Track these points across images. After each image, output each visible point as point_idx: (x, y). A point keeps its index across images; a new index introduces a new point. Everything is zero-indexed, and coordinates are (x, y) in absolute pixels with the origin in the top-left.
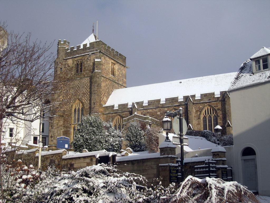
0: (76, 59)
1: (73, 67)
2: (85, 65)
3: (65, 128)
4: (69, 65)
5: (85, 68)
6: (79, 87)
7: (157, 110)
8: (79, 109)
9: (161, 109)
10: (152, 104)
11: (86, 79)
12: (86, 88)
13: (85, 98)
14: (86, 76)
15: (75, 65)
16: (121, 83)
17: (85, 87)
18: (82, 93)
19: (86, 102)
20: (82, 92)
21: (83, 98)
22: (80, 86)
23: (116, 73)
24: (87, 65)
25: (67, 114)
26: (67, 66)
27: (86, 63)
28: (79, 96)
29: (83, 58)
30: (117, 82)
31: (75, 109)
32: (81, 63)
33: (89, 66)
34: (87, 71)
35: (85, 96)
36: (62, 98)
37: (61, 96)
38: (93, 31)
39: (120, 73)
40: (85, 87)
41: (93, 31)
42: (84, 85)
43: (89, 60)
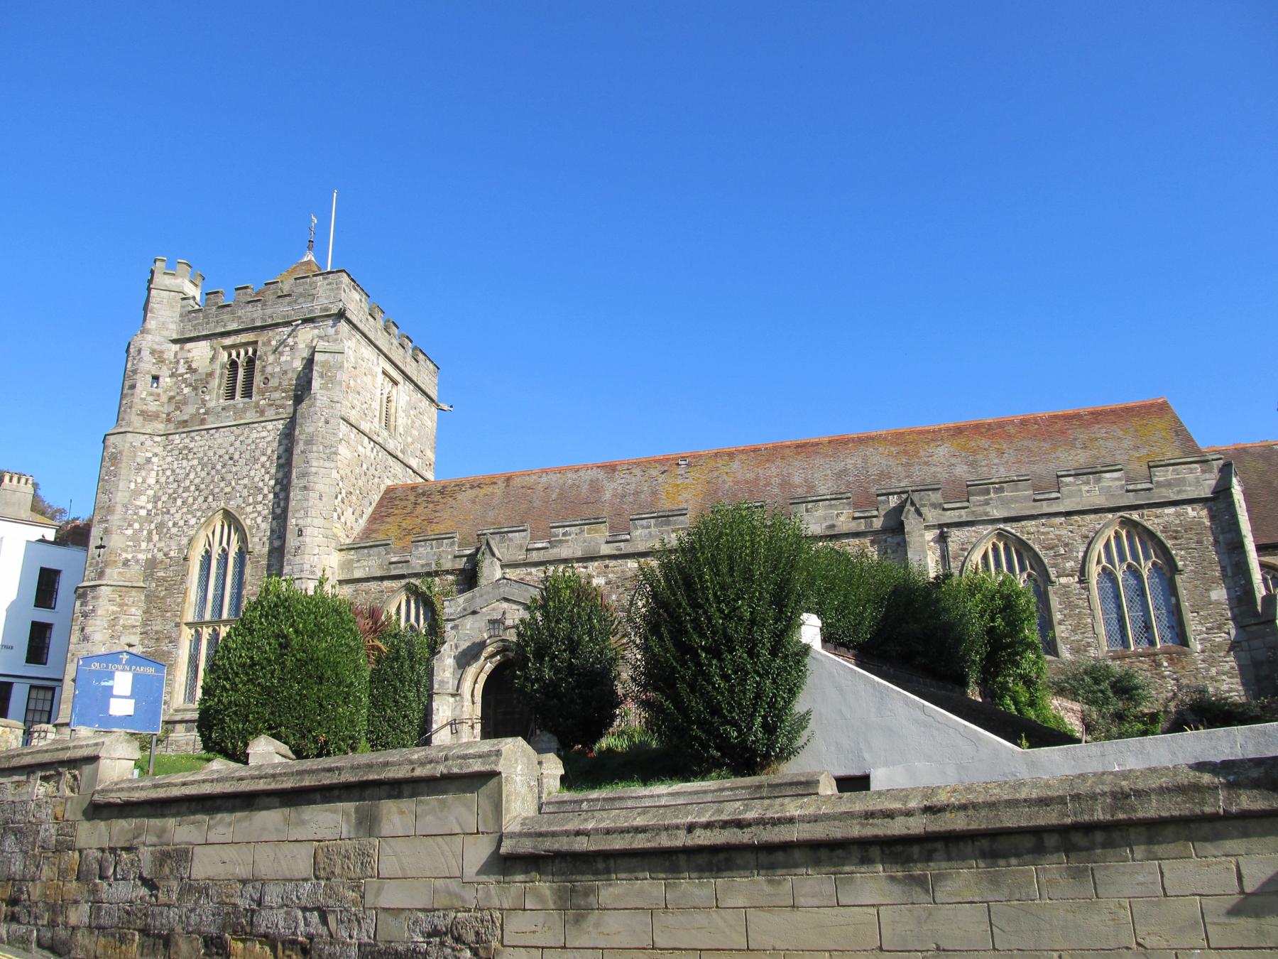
0: (228, 341)
1: (211, 375)
2: (269, 369)
3: (152, 643)
4: (194, 366)
6: (231, 459)
7: (593, 567)
9: (612, 563)
10: (567, 541)
13: (259, 508)
14: (270, 413)
15: (223, 367)
16: (414, 463)
17: (264, 459)
18: (245, 486)
20: (246, 481)
21: (249, 509)
22: (236, 456)
23: (400, 421)
24: (277, 369)
25: (164, 579)
26: (182, 370)
27: (271, 358)
29: (262, 338)
30: (400, 455)
31: (207, 556)
32: (251, 362)
33: (285, 372)
34: (277, 395)
35: (260, 498)
36: (150, 506)
37: (144, 498)
39: (413, 422)
42: (257, 453)
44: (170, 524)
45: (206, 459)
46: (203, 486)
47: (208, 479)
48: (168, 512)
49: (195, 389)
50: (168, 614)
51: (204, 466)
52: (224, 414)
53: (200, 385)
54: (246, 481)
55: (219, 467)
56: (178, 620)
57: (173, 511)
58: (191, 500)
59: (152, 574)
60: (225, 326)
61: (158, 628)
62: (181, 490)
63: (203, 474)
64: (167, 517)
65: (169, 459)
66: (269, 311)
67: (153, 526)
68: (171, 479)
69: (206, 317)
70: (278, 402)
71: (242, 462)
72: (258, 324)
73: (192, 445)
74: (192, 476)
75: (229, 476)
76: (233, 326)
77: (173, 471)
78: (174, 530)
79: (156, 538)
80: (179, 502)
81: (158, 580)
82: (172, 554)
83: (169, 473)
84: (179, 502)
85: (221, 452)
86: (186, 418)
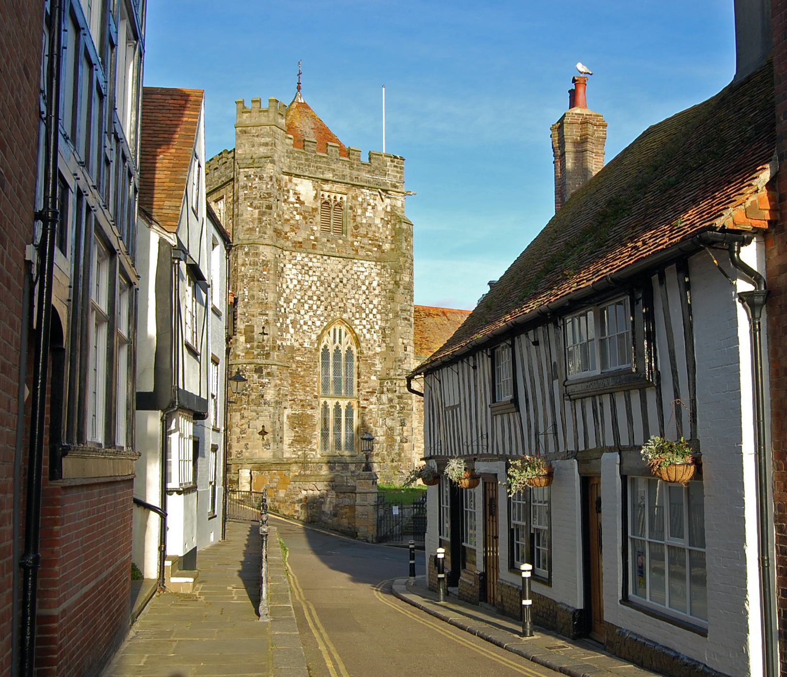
2: (358, 219)
4: (302, 199)
5: (356, 227)
8: (337, 351)
11: (366, 265)
12: (364, 293)
13: (364, 322)
19: (368, 336)
20: (353, 301)
21: (357, 322)
22: (345, 281)
26: (292, 199)
28: (345, 312)
33: (370, 225)
34: (366, 241)
35: (364, 316)
38: (299, 88)
40: (364, 288)
41: (299, 88)
43: (370, 207)
44: (302, 322)
45: (322, 278)
46: (322, 298)
47: (326, 295)
48: (299, 313)
49: (305, 218)
50: (308, 389)
51: (322, 283)
52: (329, 245)
53: (308, 215)
54: (353, 301)
55: (333, 286)
56: (316, 394)
57: (302, 312)
58: (315, 307)
59: (293, 358)
60: (323, 174)
61: (302, 398)
62: (306, 298)
63: (322, 289)
64: (298, 317)
65: (294, 271)
66: (355, 173)
67: (288, 321)
68: (298, 287)
69: (307, 160)
70: (367, 247)
71: (349, 286)
72: (347, 180)
73: (310, 264)
74: (314, 288)
75: (341, 295)
76: (329, 176)
77: (299, 282)
78: (305, 327)
79: (292, 331)
80: (306, 306)
81: (298, 362)
82: (306, 345)
83: (295, 282)
84: (306, 306)
85: (334, 275)
86: (301, 240)
